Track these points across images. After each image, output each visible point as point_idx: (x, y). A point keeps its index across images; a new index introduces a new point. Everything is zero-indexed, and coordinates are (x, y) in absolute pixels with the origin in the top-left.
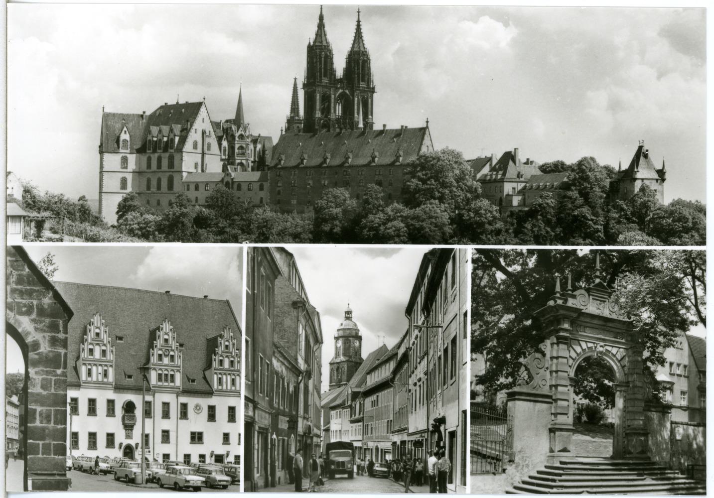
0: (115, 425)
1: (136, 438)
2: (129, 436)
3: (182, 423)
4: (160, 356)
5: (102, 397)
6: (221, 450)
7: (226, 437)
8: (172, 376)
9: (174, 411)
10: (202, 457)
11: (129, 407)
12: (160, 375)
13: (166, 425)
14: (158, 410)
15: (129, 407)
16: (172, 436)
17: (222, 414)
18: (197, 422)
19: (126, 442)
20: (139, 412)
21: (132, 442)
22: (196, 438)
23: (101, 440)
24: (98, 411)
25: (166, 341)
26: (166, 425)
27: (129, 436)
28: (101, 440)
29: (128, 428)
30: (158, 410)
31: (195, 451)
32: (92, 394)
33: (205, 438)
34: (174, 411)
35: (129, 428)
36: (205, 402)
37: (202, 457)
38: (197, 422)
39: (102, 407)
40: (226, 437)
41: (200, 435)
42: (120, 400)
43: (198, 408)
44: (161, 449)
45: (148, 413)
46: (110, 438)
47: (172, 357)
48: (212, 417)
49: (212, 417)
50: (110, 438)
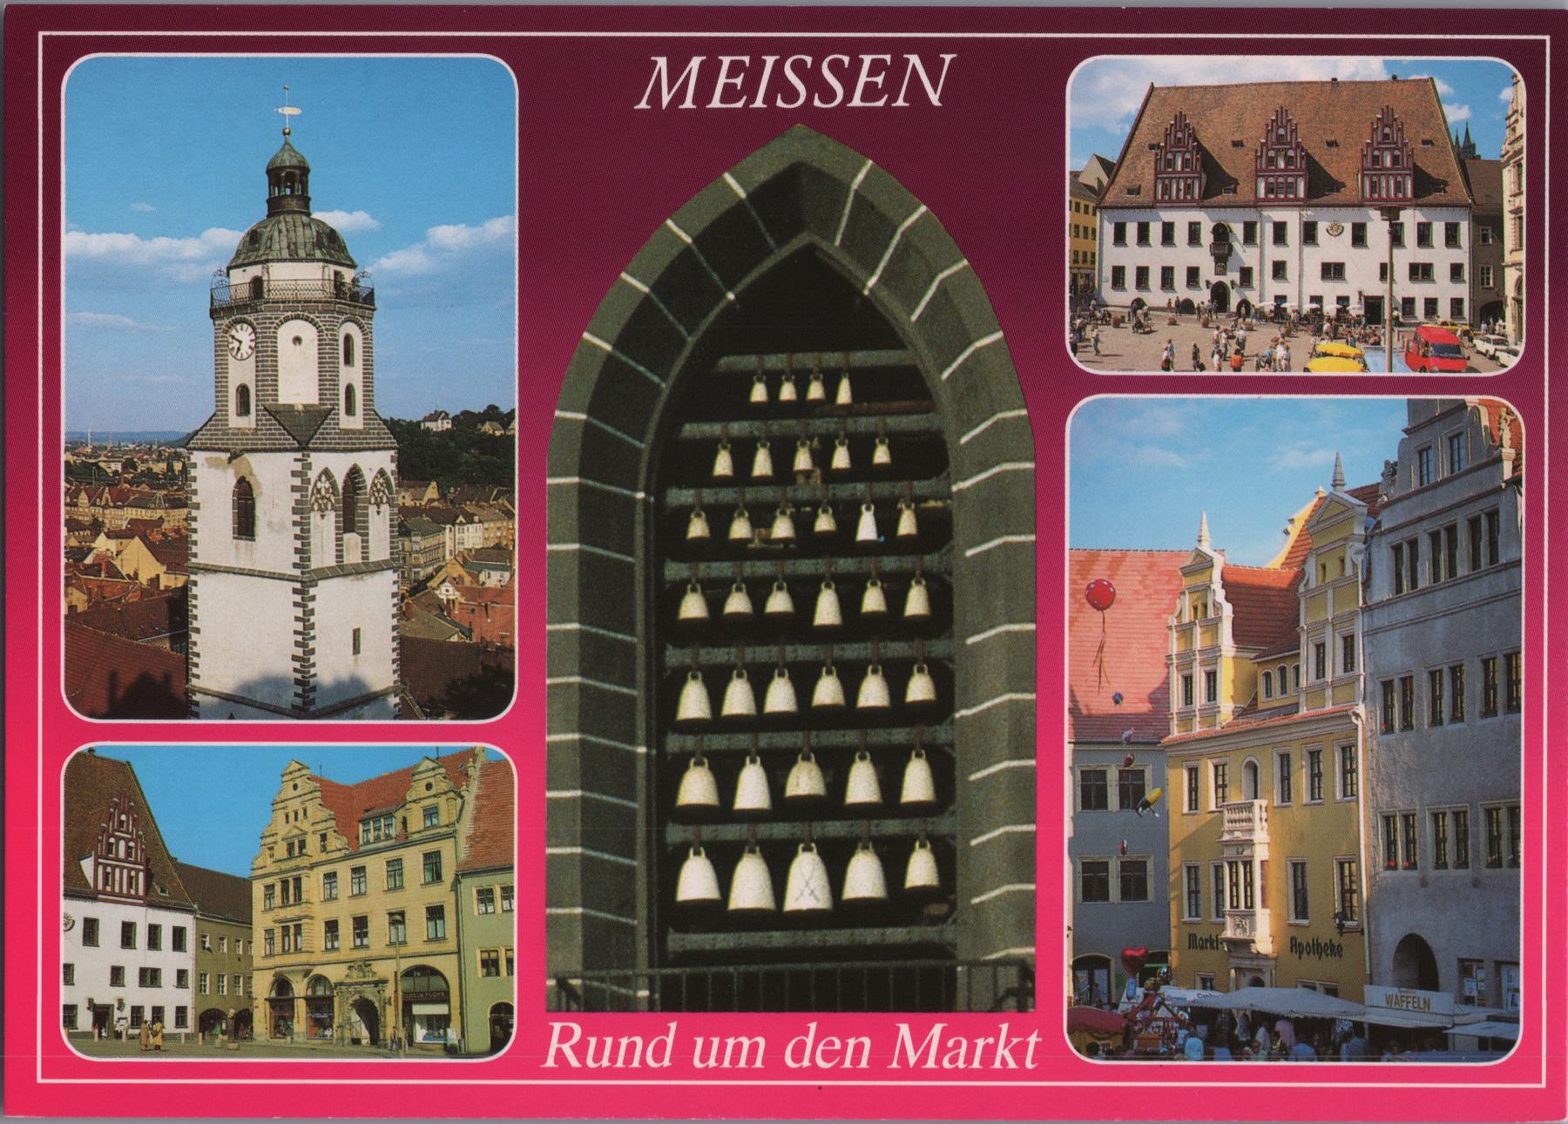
3: (1308, 250)
5: (1181, 219)
6: (1376, 288)
7: (1385, 271)
9: (1294, 233)
10: (1343, 300)
11: (1221, 233)
16: (1292, 270)
18: (1332, 246)
19: (1214, 279)
21: (1226, 279)
22: (1333, 271)
23: (1180, 278)
24: (1176, 239)
28: (1180, 278)
31: (1330, 291)
32: (1167, 216)
33: (1348, 271)
34: (1294, 233)
37: (1343, 300)
38: (1332, 246)
39: (1181, 234)
44: (1274, 288)
45: (1249, 237)
46: (1193, 274)
48: (1359, 238)
49: (1359, 238)
50: (1193, 274)
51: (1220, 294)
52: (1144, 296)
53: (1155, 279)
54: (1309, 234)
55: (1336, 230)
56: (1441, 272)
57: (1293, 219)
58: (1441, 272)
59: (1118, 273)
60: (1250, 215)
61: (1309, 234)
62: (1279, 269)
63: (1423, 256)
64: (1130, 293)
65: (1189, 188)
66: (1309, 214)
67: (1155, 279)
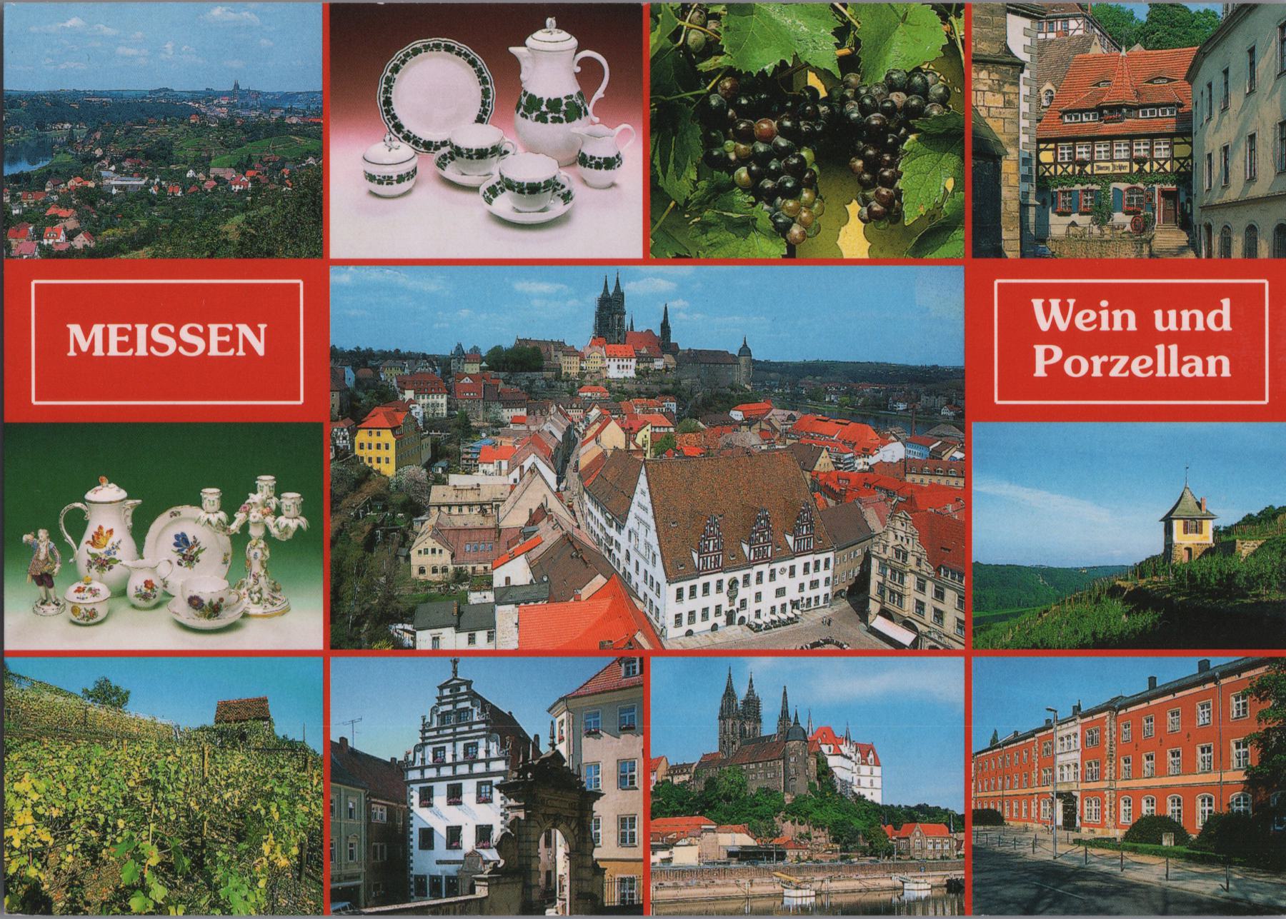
1: (737, 604)
5: (712, 579)
13: (759, 588)
14: (753, 579)
17: (799, 570)
18: (782, 580)
19: (729, 609)
21: (734, 608)
26: (759, 588)
29: (732, 599)
30: (753, 579)
35: (732, 599)
36: (787, 564)
38: (782, 580)
42: (726, 577)
43: (783, 571)
50: (718, 609)
52: (694, 628)
53: (698, 616)
54: (772, 575)
56: (822, 583)
57: (765, 569)
58: (822, 583)
59: (678, 616)
61: (772, 575)
62: (758, 596)
64: (686, 626)
65: (717, 560)
67: (698, 616)
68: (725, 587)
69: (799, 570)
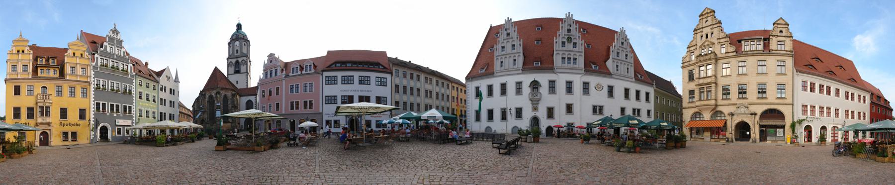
0: (523, 101)
2: (535, 109)
4: (563, 43)
8: (575, 59)
9: (578, 87)
12: (563, 58)
13: (569, 99)
14: (561, 87)
15: (535, 85)
16: (575, 109)
17: (619, 92)
20: (544, 89)
25: (569, 31)
27: (535, 109)
30: (561, 87)
34: (578, 87)
35: (535, 103)
36: (605, 82)
40: (623, 110)
41: (601, 108)
42: (527, 79)
47: (575, 44)
51: (535, 121)
55: (599, 87)
56: (644, 113)
57: (578, 81)
60: (552, 77)
62: (569, 108)
63: (637, 105)
66: (587, 78)
68: (526, 90)
69: (619, 92)
